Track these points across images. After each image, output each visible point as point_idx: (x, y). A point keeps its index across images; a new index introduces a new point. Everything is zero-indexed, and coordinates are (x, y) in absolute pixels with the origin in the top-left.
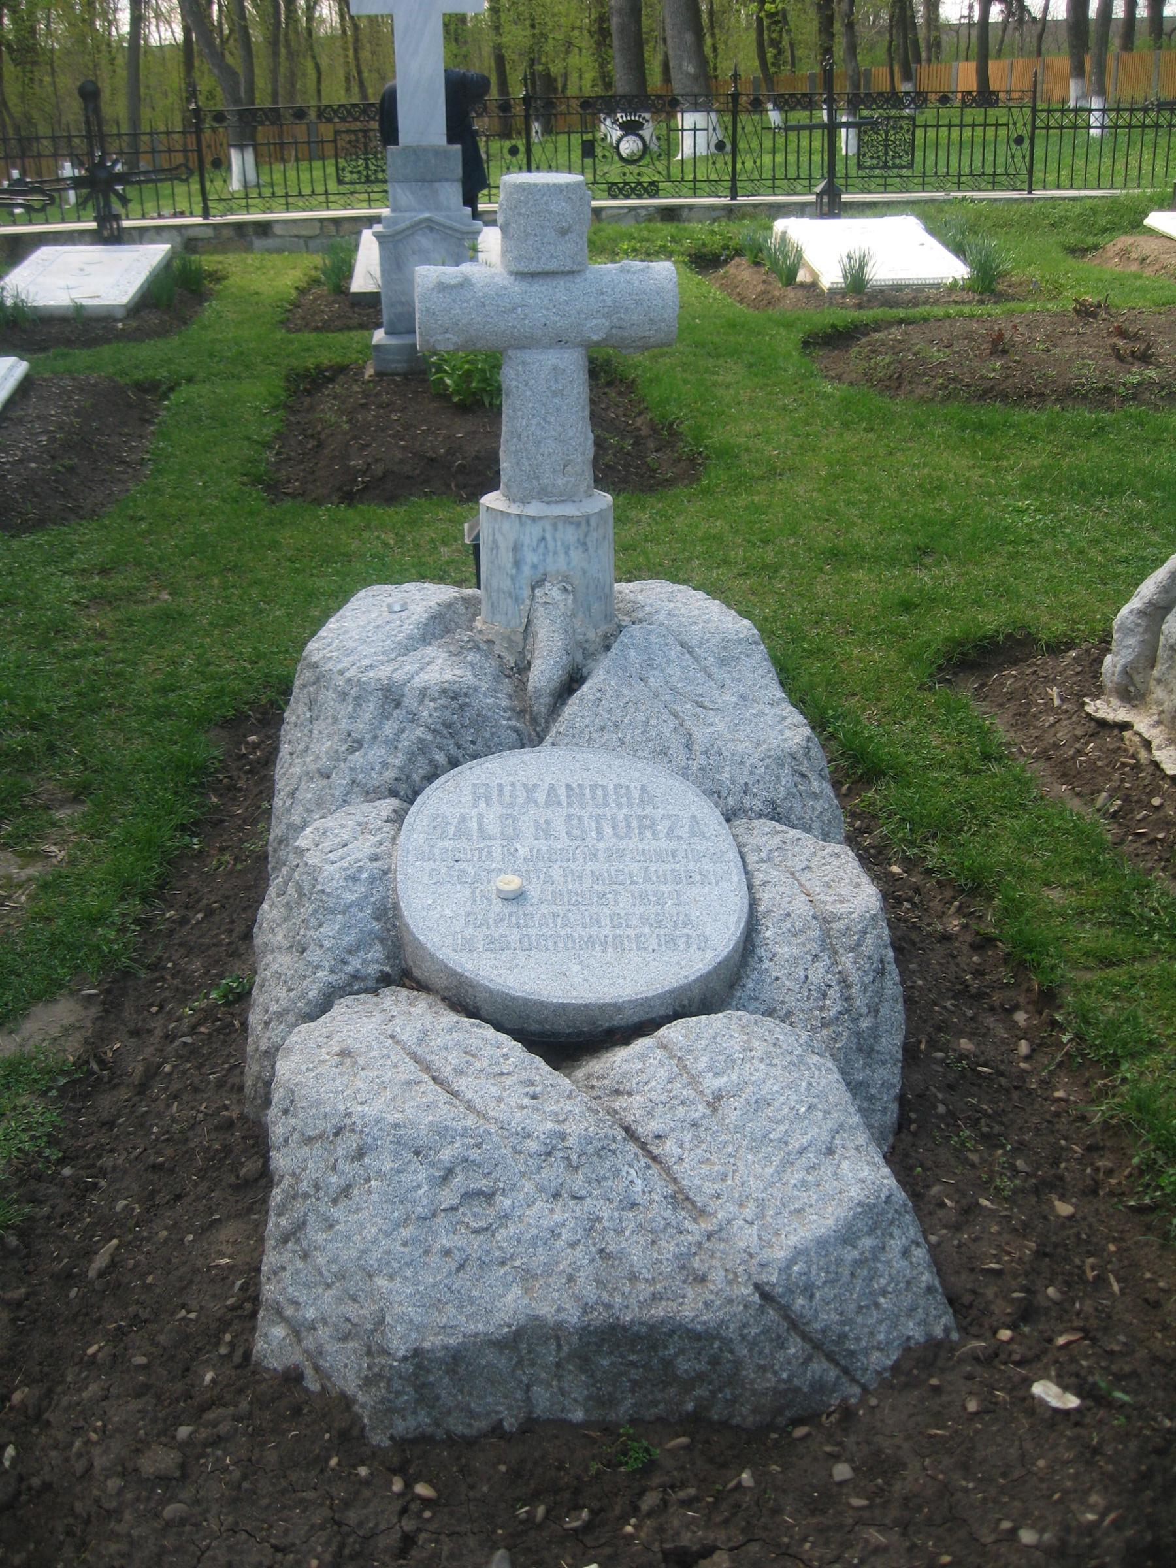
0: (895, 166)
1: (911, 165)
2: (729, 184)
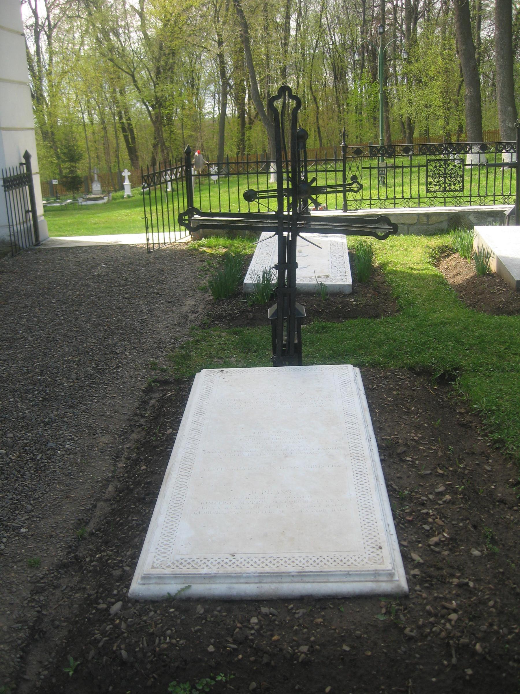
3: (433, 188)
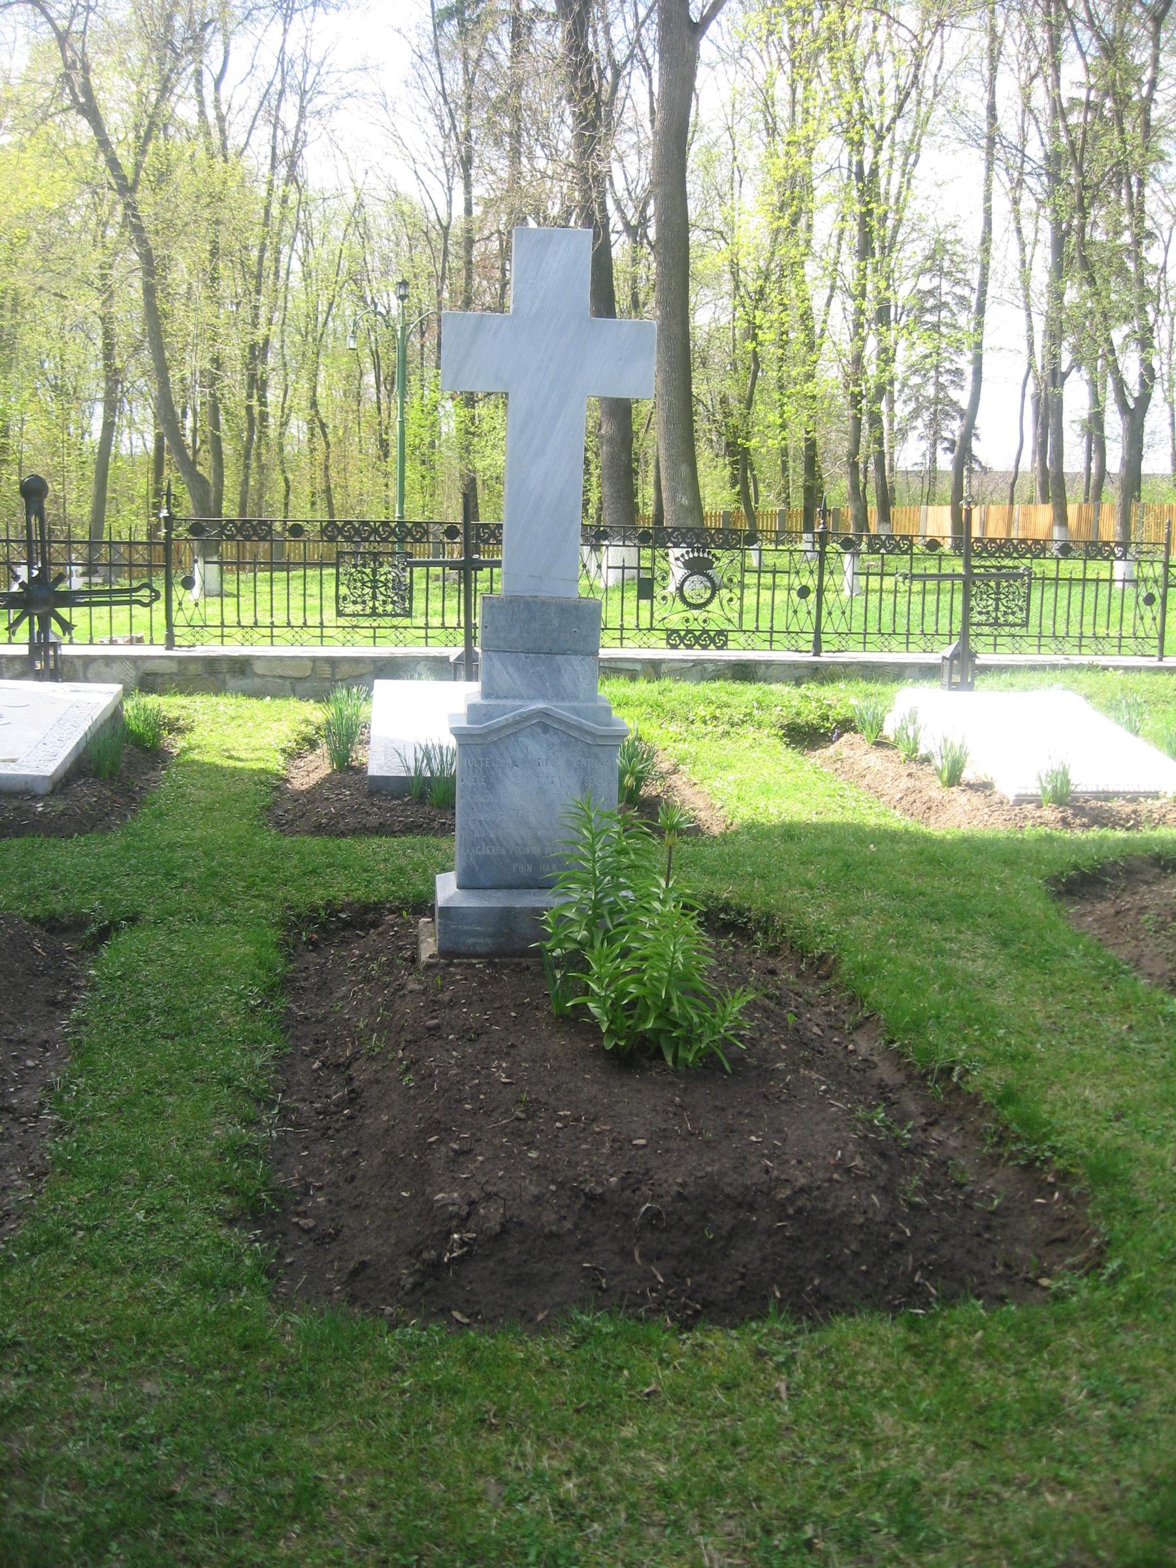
0: (1007, 624)
1: (1025, 624)
2: (811, 637)
3: (350, 608)
